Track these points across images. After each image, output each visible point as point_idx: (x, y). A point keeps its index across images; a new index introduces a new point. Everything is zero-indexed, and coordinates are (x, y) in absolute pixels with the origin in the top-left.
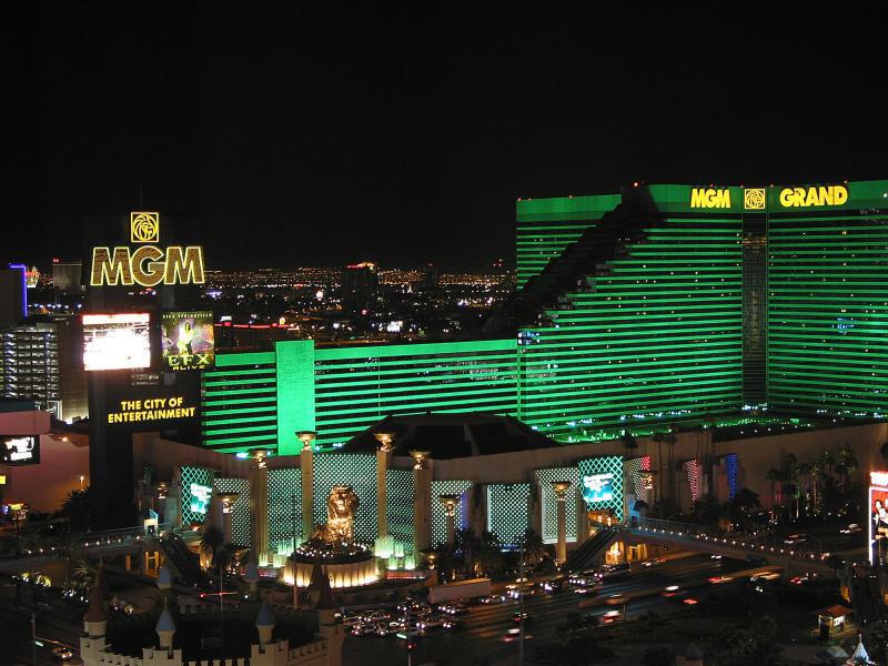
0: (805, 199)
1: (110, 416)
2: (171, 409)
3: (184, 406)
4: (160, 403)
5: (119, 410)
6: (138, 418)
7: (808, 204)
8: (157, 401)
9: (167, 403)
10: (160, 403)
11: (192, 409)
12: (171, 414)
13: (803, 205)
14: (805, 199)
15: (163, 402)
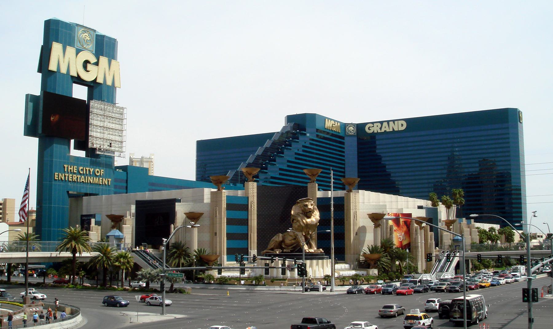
0: (381, 129)
1: (56, 174)
2: (96, 176)
3: (105, 176)
4: (89, 170)
5: (62, 170)
6: (75, 179)
7: (383, 131)
8: (88, 169)
9: (94, 172)
10: (89, 170)
11: (110, 180)
12: (96, 180)
13: (379, 131)
14: (381, 129)
15: (92, 170)
